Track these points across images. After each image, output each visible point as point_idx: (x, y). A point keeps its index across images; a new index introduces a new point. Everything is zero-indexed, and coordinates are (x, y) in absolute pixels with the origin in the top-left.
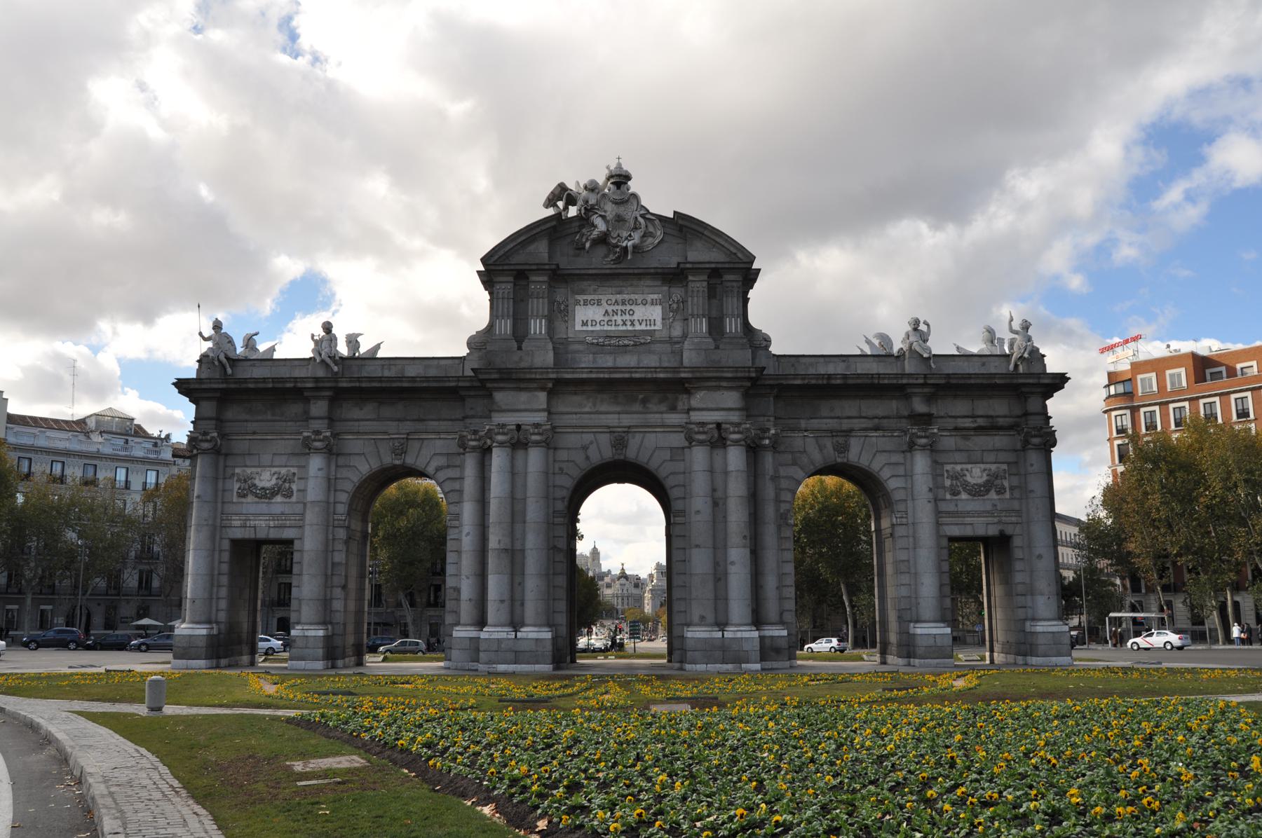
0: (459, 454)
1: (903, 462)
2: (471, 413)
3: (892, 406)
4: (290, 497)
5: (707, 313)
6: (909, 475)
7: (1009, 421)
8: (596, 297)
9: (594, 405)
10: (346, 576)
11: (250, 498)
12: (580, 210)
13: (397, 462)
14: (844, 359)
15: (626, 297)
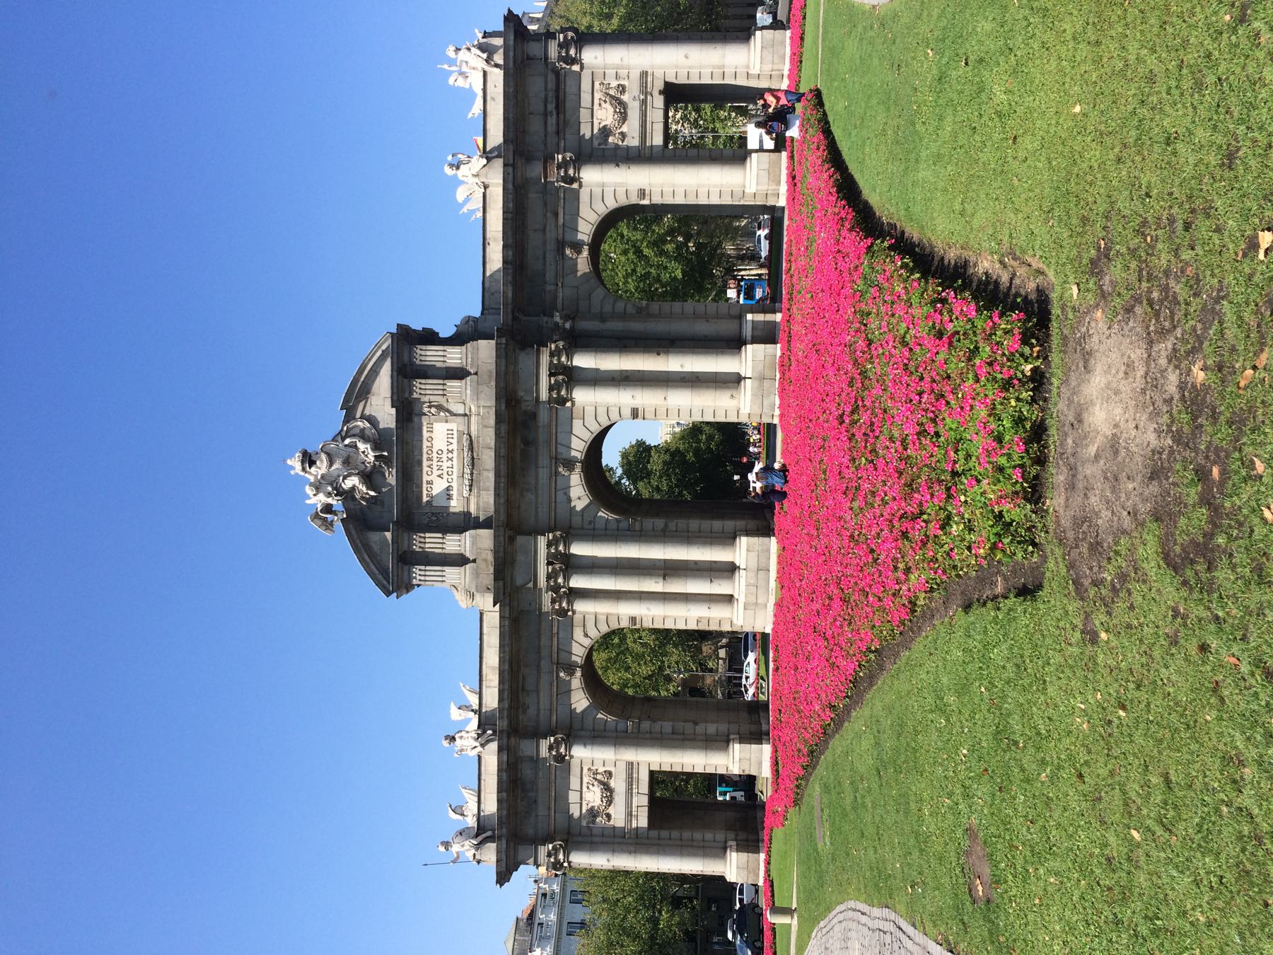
5: (441, 382)
7: (551, 77)
8: (425, 485)
9: (528, 490)
10: (685, 721)
11: (611, 810)
15: (425, 456)
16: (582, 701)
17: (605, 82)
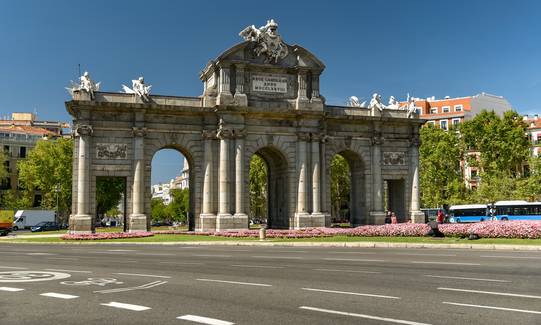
0: (200, 140)
1: (369, 150)
2: (208, 123)
3: (367, 128)
4: (124, 157)
6: (372, 155)
7: (406, 136)
9: (261, 122)
11: (105, 157)
12: (257, 39)
13: (174, 143)
16: (160, 144)
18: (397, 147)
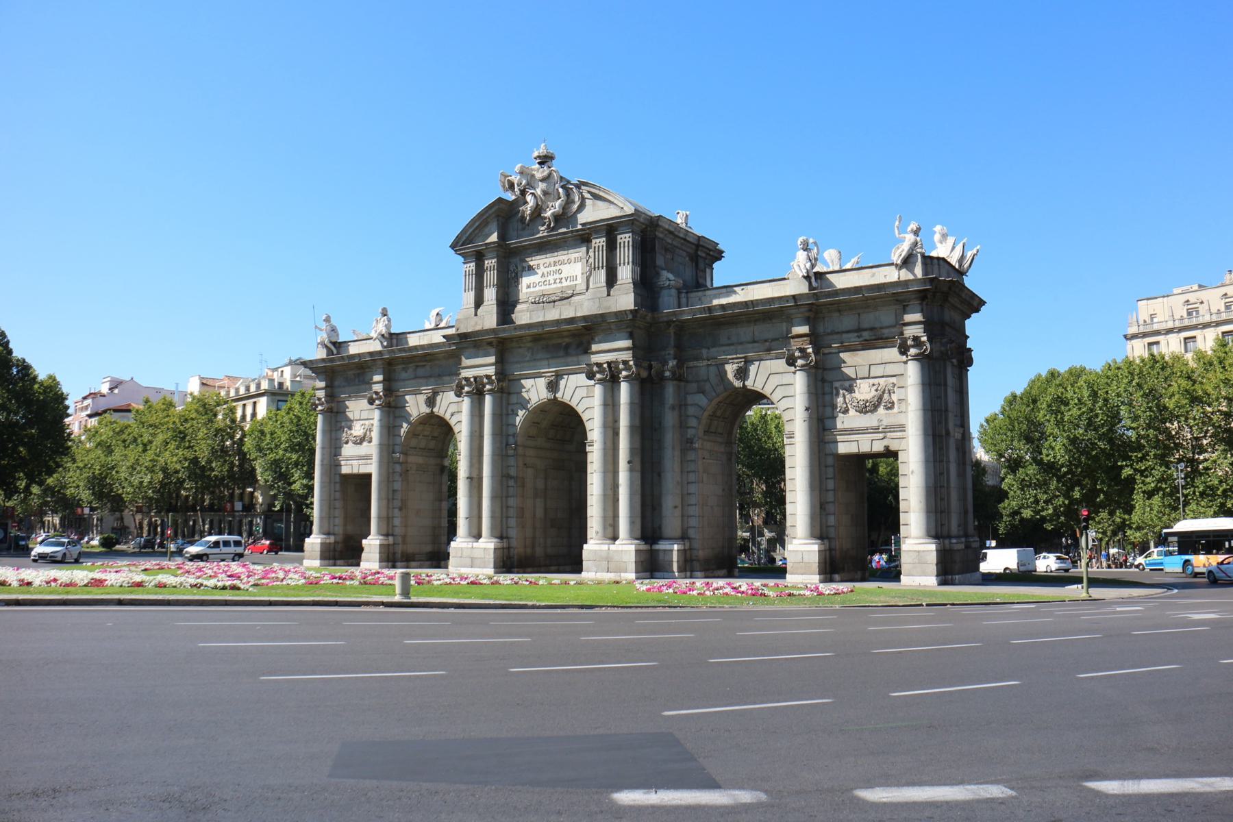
5: (605, 265)
9: (532, 354)
14: (742, 287)
17: (895, 388)
18: (870, 365)
